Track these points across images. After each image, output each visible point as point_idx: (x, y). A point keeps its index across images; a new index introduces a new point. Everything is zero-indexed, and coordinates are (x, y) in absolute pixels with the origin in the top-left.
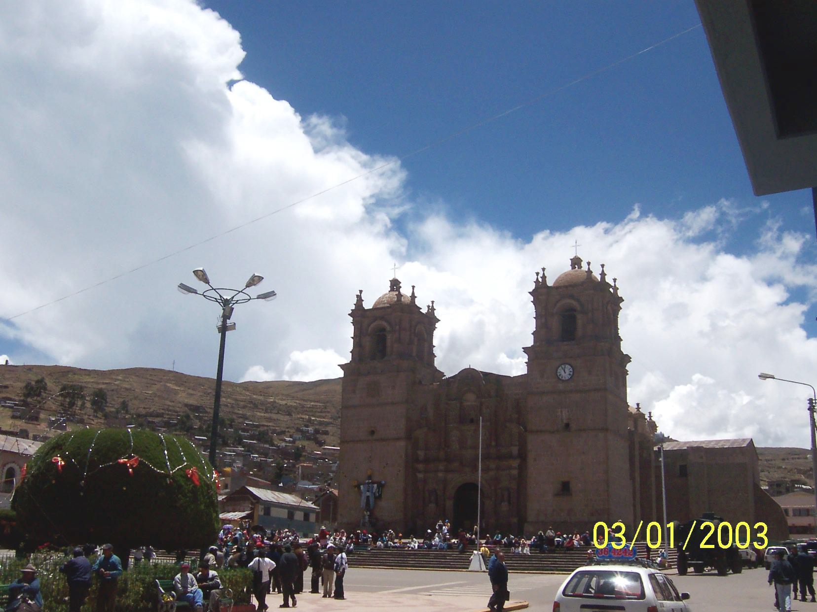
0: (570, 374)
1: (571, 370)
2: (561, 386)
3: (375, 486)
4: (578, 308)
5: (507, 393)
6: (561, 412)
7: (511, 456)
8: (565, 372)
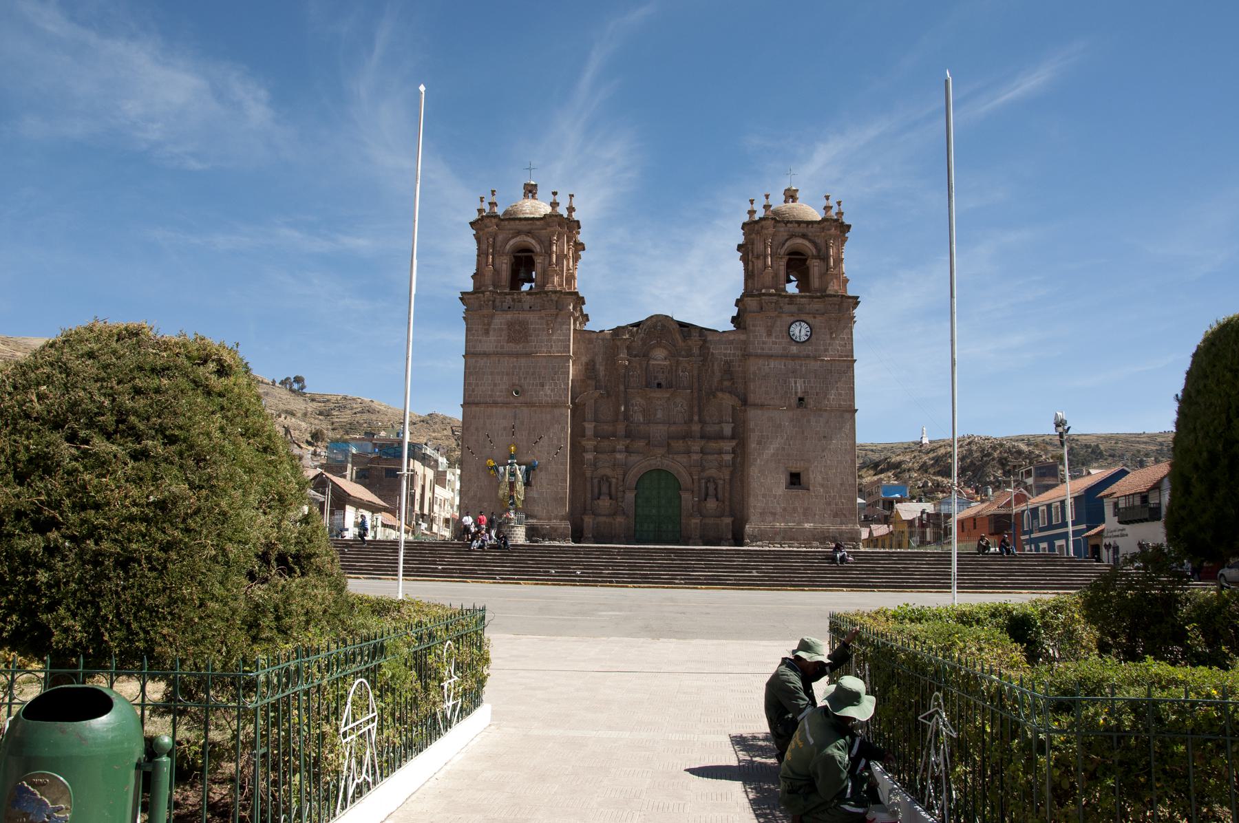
0: (807, 335)
1: (808, 329)
3: (523, 467)
6: (796, 383)
7: (720, 437)
8: (800, 331)
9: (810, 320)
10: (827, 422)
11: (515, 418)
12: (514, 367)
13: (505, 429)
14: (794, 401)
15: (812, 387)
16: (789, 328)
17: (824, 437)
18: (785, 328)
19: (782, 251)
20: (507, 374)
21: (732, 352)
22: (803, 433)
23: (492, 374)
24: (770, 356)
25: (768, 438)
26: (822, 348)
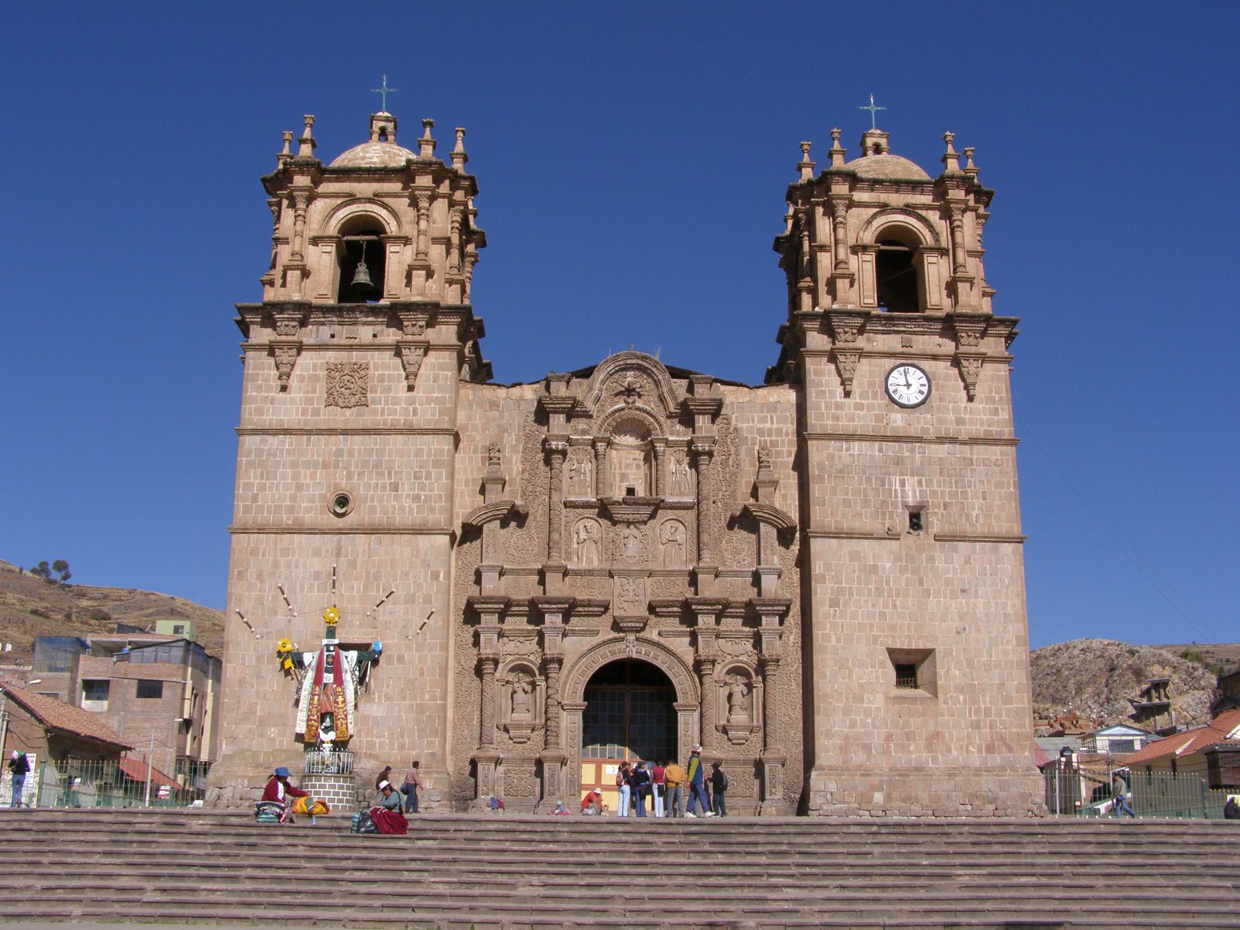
0: (921, 392)
1: (924, 381)
2: (898, 420)
3: (353, 655)
4: (927, 238)
5: (739, 425)
6: (903, 484)
9: (925, 364)
10: (967, 561)
11: (338, 554)
12: (339, 452)
13: (317, 575)
14: (901, 521)
15: (935, 492)
16: (887, 378)
17: (963, 591)
18: (879, 380)
19: (868, 237)
20: (325, 466)
21: (775, 426)
22: (921, 583)
23: (294, 465)
24: (849, 437)
25: (851, 594)
26: (951, 417)
